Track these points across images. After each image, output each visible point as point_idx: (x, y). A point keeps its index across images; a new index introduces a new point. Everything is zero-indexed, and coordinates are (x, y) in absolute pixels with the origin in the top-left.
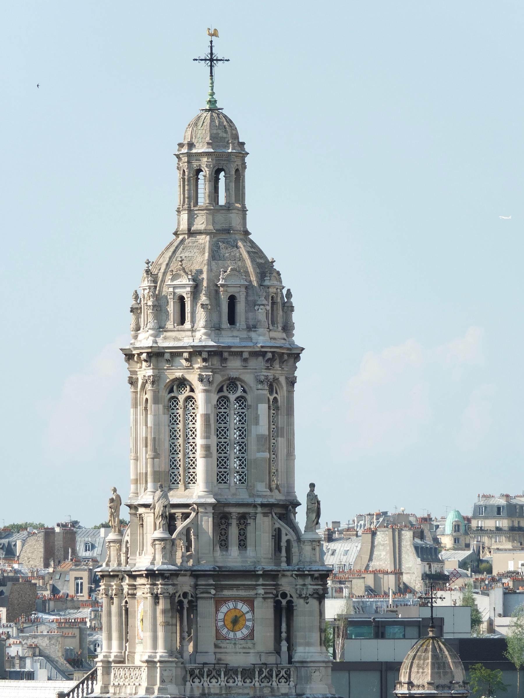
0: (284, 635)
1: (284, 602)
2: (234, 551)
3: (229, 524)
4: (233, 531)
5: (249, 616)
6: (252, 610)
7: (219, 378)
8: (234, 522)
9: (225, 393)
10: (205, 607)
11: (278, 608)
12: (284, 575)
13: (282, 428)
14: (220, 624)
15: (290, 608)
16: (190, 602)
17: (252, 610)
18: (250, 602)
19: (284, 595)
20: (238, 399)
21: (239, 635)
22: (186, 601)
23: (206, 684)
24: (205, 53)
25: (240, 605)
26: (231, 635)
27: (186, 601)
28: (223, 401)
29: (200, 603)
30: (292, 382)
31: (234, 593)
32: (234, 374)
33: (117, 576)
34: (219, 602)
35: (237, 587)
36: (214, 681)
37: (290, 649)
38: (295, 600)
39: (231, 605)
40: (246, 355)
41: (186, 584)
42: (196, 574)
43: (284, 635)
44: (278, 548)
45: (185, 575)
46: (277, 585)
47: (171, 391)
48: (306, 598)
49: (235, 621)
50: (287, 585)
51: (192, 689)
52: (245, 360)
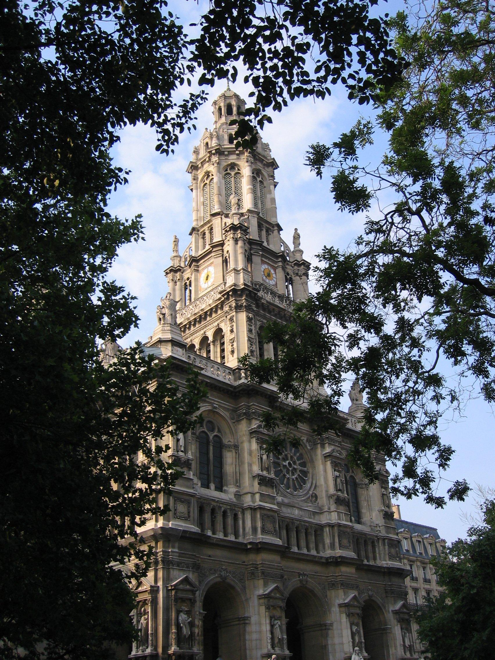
1: (288, 277)
5: (274, 275)
6: (276, 273)
12: (288, 264)
17: (276, 273)
18: (275, 269)
19: (288, 274)
20: (260, 181)
26: (267, 281)
29: (253, 257)
33: (179, 270)
35: (269, 259)
38: (293, 278)
39: (266, 266)
47: (227, 170)
52: (264, 165)
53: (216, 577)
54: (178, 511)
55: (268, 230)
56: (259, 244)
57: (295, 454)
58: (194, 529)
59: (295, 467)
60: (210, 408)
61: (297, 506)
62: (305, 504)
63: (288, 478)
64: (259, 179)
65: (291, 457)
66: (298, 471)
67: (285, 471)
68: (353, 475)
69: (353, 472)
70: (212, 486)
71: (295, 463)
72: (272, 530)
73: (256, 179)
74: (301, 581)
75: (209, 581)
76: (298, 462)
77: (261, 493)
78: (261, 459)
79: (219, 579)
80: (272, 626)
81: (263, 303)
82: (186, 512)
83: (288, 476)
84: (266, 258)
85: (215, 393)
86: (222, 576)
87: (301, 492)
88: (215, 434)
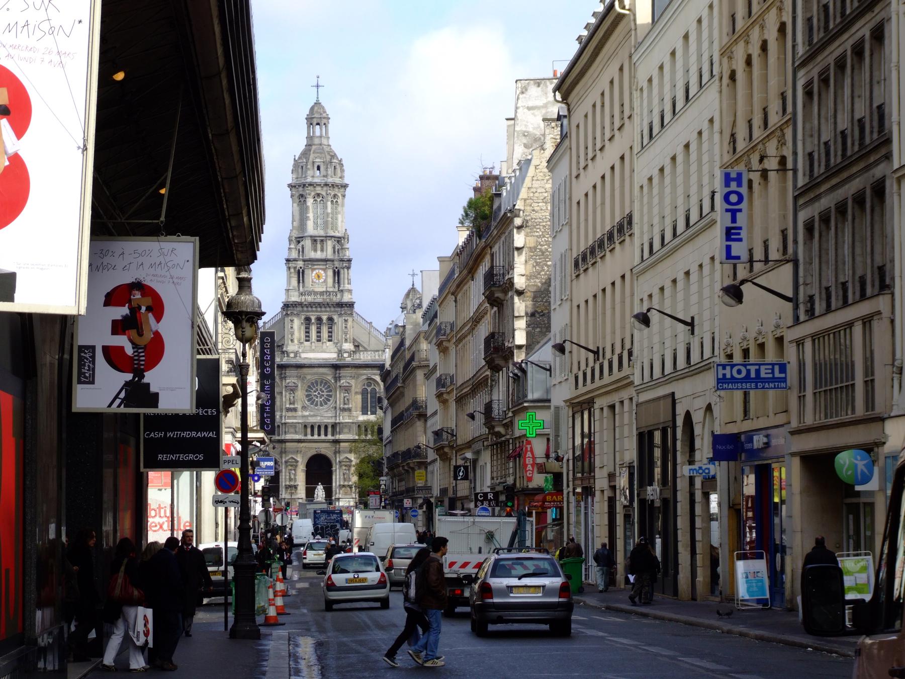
2: (319, 253)
4: (319, 246)
7: (313, 194)
11: (334, 272)
15: (339, 272)
24: (315, 84)
30: (344, 196)
34: (313, 270)
37: (339, 286)
41: (300, 264)
42: (304, 261)
44: (334, 252)
49: (319, 277)
50: (337, 264)
56: (311, 260)
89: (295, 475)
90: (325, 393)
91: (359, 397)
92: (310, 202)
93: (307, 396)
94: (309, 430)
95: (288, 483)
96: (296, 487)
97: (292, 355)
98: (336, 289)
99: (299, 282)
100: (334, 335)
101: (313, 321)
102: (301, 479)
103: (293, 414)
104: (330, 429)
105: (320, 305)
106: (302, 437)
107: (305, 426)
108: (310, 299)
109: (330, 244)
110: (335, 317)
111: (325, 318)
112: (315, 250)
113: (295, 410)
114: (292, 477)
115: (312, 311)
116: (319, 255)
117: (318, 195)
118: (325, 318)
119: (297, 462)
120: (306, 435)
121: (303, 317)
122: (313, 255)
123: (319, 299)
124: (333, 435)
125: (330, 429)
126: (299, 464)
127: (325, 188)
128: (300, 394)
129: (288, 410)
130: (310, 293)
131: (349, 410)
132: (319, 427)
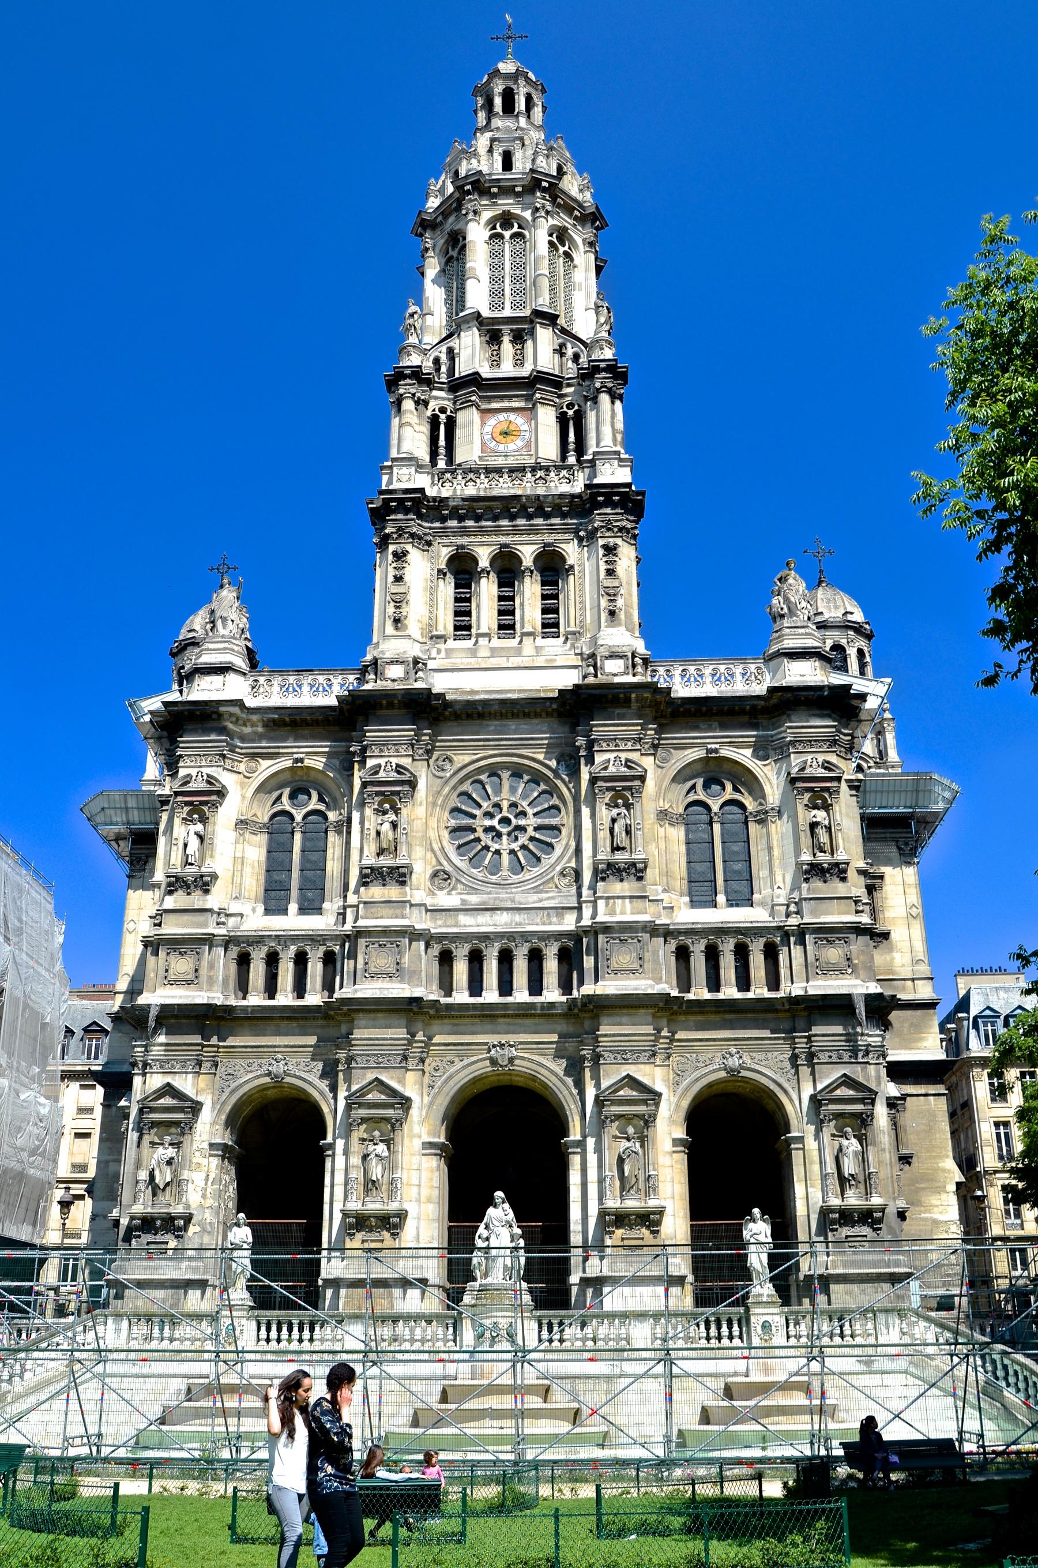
0: (572, 446)
1: (571, 413)
3: (500, 343)
4: (507, 348)
7: (487, 215)
8: (506, 340)
9: (499, 230)
10: (469, 420)
11: (562, 420)
12: (569, 385)
13: (580, 284)
14: (487, 437)
15: (579, 418)
16: (449, 418)
20: (514, 236)
21: (512, 447)
22: (443, 417)
23: (459, 487)
25: (512, 417)
26: (501, 447)
27: (443, 417)
28: (496, 237)
31: (506, 404)
32: (506, 208)
36: (471, 484)
39: (501, 417)
40: (519, 189)
41: (439, 399)
42: (456, 386)
43: (572, 446)
45: (441, 389)
46: (561, 396)
48: (595, 400)
51: (439, 491)
53: (258, 1077)
54: (171, 971)
55: (518, 338)
56: (474, 380)
57: (524, 796)
58: (217, 997)
59: (522, 822)
60: (289, 763)
61: (509, 905)
62: (535, 897)
63: (498, 852)
64: (507, 234)
65: (513, 805)
66: (530, 832)
67: (486, 839)
68: (737, 796)
69: (736, 789)
70: (293, 907)
71: (524, 814)
72: (392, 970)
73: (500, 236)
74: (493, 1062)
75: (241, 1086)
76: (530, 811)
77: (365, 903)
78: (378, 833)
79: (267, 1080)
80: (365, 1157)
81: (456, 508)
82: (192, 971)
83: (494, 846)
84: (502, 398)
85: (306, 732)
86: (269, 1074)
87: (537, 871)
88: (311, 807)
89: (390, 1163)
90: (531, 822)
91: (677, 834)
92: (477, 233)
93: (455, 831)
94: (461, 969)
95: (354, 1205)
96: (391, 1223)
97: (395, 672)
98: (572, 460)
99: (434, 454)
100: (569, 617)
101: (484, 562)
102: (421, 1184)
103: (392, 892)
104: (551, 966)
105: (507, 508)
106: (427, 991)
107: (446, 959)
108: (471, 491)
109: (545, 336)
110: (571, 551)
111: (528, 553)
112: (496, 362)
113: (400, 876)
114: (377, 1171)
115: (483, 531)
116: (507, 369)
117: (506, 220)
118: (528, 553)
119: (405, 1103)
120: (447, 987)
121: (445, 552)
122: (486, 372)
123: (504, 487)
124: (566, 986)
125: (551, 966)
126: (415, 1112)
127: (528, 199)
128: (425, 818)
129: (371, 876)
130: (472, 472)
131: (636, 871)
132: (506, 958)
